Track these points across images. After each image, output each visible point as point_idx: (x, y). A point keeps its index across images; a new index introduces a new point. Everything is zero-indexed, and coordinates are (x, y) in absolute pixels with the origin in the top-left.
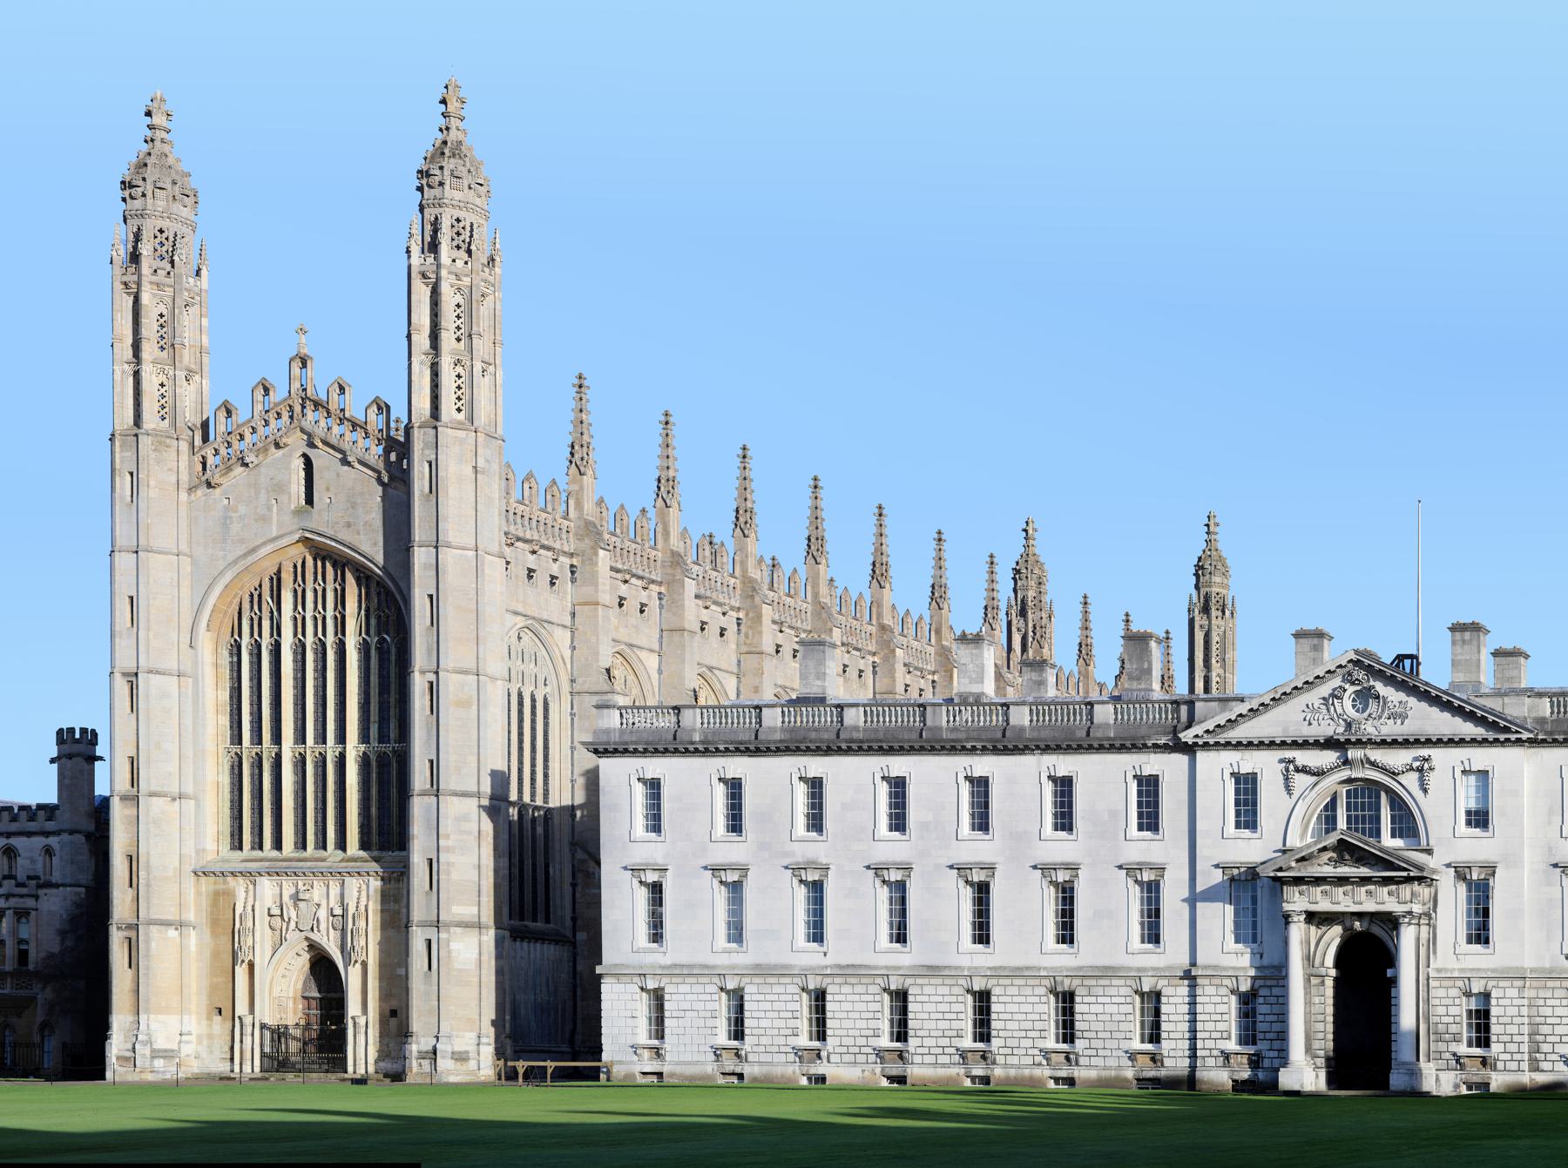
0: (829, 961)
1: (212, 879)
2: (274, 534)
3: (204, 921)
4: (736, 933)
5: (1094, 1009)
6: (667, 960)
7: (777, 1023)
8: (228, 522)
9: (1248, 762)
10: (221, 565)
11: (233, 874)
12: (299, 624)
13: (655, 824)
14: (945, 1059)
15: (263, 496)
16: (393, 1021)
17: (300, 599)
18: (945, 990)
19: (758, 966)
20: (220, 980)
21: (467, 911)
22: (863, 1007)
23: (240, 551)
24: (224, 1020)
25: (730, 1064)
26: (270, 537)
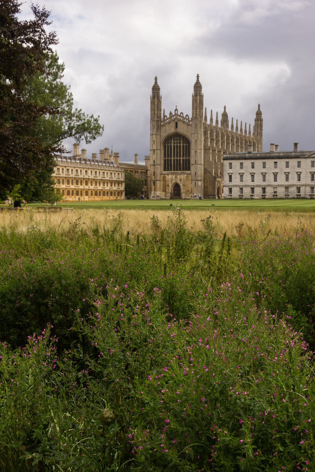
4: (241, 181)
12: (174, 143)
17: (174, 140)
21: (200, 178)
23: (167, 134)
25: (241, 197)
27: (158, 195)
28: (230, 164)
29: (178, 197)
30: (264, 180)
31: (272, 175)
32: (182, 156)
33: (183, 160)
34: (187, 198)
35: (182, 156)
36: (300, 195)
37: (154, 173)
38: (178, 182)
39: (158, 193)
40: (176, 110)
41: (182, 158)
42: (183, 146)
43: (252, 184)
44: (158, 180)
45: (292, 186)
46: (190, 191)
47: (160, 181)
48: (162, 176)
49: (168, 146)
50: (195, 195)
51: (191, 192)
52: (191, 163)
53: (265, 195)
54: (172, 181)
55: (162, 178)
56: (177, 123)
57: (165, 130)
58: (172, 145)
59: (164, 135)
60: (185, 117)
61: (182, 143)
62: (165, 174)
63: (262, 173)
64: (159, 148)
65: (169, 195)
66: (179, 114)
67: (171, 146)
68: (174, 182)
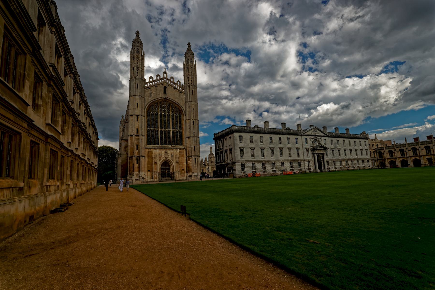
0: (265, 160)
1: (148, 149)
2: (160, 97)
5: (295, 164)
6: (245, 160)
7: (260, 168)
9: (307, 137)
11: (152, 148)
12: (161, 111)
13: (241, 141)
14: (279, 171)
15: (158, 91)
16: (183, 171)
18: (279, 163)
19: (257, 160)
20: (150, 166)
22: (270, 165)
23: (153, 99)
24: (150, 172)
28: (241, 137)
29: (170, 179)
30: (272, 156)
31: (279, 150)
32: (171, 127)
33: (173, 132)
34: (181, 178)
35: (171, 127)
36: (301, 169)
37: (137, 146)
38: (169, 158)
39: (142, 173)
41: (171, 130)
42: (173, 116)
43: (263, 159)
44: (143, 156)
45: (294, 161)
46: (185, 170)
47: (144, 157)
49: (153, 115)
50: (196, 174)
51: (189, 170)
52: (184, 136)
53: (275, 171)
54: (160, 157)
56: (165, 88)
57: (151, 94)
58: (159, 114)
59: (149, 100)
61: (171, 112)
63: (270, 148)
64: (143, 115)
68: (163, 158)
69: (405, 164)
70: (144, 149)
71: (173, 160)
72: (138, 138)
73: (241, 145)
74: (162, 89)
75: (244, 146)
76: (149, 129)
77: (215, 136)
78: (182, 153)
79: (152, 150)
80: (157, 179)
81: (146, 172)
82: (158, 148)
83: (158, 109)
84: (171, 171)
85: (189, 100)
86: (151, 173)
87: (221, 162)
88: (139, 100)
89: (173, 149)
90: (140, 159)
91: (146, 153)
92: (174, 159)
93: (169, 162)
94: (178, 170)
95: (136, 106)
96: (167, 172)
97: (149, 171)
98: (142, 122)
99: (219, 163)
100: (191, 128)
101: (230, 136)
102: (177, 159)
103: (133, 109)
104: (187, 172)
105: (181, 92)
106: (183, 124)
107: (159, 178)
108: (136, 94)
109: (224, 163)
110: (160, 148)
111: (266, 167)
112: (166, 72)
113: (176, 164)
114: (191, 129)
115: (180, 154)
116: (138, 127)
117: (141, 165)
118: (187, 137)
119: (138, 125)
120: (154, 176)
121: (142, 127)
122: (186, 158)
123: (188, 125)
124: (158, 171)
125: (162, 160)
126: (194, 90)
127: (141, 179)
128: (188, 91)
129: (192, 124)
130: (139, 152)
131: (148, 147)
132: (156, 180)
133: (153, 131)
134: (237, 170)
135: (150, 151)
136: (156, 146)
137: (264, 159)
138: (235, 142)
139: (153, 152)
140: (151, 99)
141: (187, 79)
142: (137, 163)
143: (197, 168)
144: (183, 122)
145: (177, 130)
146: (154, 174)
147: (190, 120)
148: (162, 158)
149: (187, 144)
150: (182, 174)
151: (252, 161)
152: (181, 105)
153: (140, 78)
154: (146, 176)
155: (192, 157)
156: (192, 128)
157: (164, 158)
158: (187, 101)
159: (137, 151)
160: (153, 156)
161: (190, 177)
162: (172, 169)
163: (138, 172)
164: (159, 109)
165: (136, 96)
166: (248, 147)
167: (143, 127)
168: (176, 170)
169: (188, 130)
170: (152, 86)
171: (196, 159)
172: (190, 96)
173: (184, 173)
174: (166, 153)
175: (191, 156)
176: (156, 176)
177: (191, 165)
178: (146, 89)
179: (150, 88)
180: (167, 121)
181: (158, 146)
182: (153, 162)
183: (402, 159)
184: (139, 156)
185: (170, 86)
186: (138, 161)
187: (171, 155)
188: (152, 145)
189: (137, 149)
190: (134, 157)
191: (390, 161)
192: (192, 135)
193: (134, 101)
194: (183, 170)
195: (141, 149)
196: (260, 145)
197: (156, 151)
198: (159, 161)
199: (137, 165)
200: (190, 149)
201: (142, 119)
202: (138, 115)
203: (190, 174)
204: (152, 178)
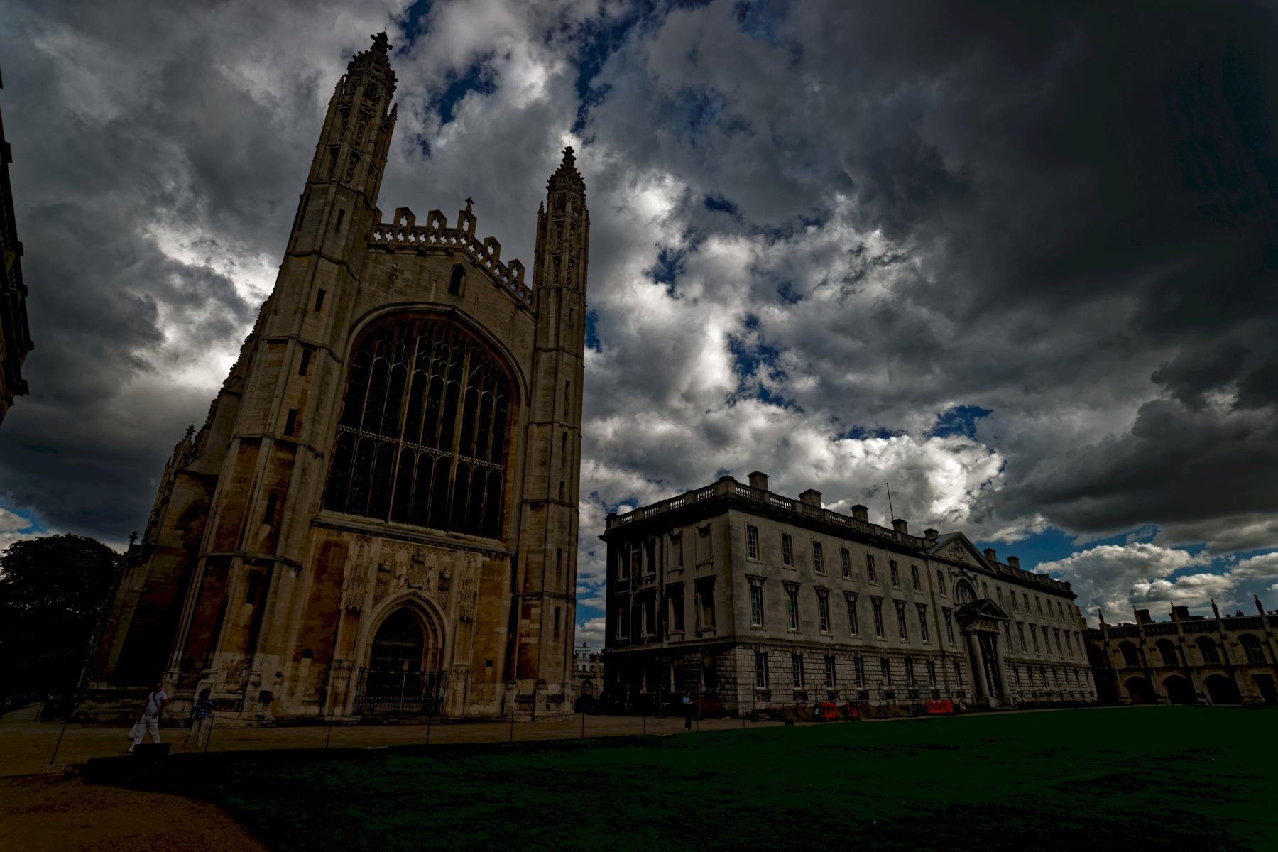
1: (325, 531)
2: (431, 300)
3: (309, 566)
6: (767, 635)
8: (394, 277)
10: (382, 302)
11: (351, 530)
12: (421, 364)
15: (425, 276)
16: (489, 670)
17: (426, 347)
22: (848, 667)
23: (400, 299)
24: (315, 661)
26: (426, 300)
27: (264, 687)
33: (463, 467)
40: (467, 215)
42: (471, 396)
46: (500, 665)
47: (298, 568)
48: (319, 536)
49: (382, 367)
50: (553, 689)
52: (512, 498)
55: (313, 551)
56: (458, 272)
57: (391, 278)
60: (505, 259)
61: (465, 379)
62: (340, 529)
64: (339, 354)
65: (347, 684)
66: (480, 236)
67: (400, 374)
68: (397, 591)
69: (1181, 691)
70: (307, 525)
71: (445, 607)
72: (290, 457)
73: (755, 568)
74: (447, 273)
75: (763, 572)
76: (347, 429)
77: (614, 525)
78: (496, 578)
79: (346, 537)
80: (345, 704)
81: (291, 657)
82: (381, 535)
83: (411, 352)
84: (427, 665)
85: (551, 345)
86: (319, 668)
87: (641, 642)
88: (333, 282)
89: (456, 547)
90: (274, 575)
91: (312, 550)
92: (454, 600)
93: (425, 619)
94: (468, 663)
95: (313, 302)
96: (406, 667)
97: (307, 653)
98: (328, 384)
99: (625, 643)
100: (554, 461)
101: (703, 524)
102: (469, 603)
103: (296, 312)
104: (507, 678)
105: (520, 307)
106: (514, 440)
107: (357, 699)
108: (325, 251)
109: (656, 646)
110: (390, 536)
111: (838, 677)
112: (473, 213)
113: (460, 628)
114: (553, 468)
115: (482, 581)
116: (303, 401)
117: (272, 612)
118: (524, 502)
119: (304, 392)
120: (329, 689)
121: (321, 411)
122: (507, 604)
123: (536, 445)
124: (360, 662)
125: (392, 597)
126: (576, 308)
127: (253, 699)
128: (553, 307)
129: (557, 443)
130: (273, 537)
131: (328, 521)
132: (338, 711)
133: (367, 444)
134: (739, 681)
135: (336, 545)
136: (371, 523)
137: (829, 641)
138: (733, 552)
139: (351, 552)
140: (386, 298)
141: (552, 265)
142: (249, 599)
143: (563, 657)
144: (516, 433)
145: (481, 462)
146: (332, 673)
147: (548, 428)
148: (391, 589)
149: (525, 531)
150: (481, 686)
151: (791, 645)
152: (516, 357)
153: (359, 192)
154: (286, 684)
155: (546, 598)
156: (556, 463)
157: (405, 591)
158: (541, 344)
159: (266, 530)
160: (347, 573)
161: (525, 706)
162: (430, 656)
163: (239, 657)
164: (416, 354)
165: (323, 262)
166: (778, 578)
167: (325, 412)
168: (455, 663)
169: (536, 471)
170: (404, 248)
171: (563, 614)
172: (558, 328)
173: (493, 681)
174: (417, 566)
175: (540, 596)
176: (341, 685)
177: (533, 640)
178: (373, 250)
179: (391, 252)
180: (441, 413)
181: (379, 524)
182: (342, 606)
183: (1169, 674)
184: (270, 557)
185: (479, 269)
186: (258, 589)
187: (441, 576)
188: (350, 512)
189: (269, 518)
190: (237, 563)
191: (1129, 677)
192: (554, 494)
193: (309, 278)
194: (490, 663)
195: (292, 519)
196: (815, 577)
197: (366, 547)
198: (377, 600)
199: (249, 608)
200: (540, 558)
201: (327, 371)
202: (315, 348)
203: (527, 687)
204: (316, 698)
